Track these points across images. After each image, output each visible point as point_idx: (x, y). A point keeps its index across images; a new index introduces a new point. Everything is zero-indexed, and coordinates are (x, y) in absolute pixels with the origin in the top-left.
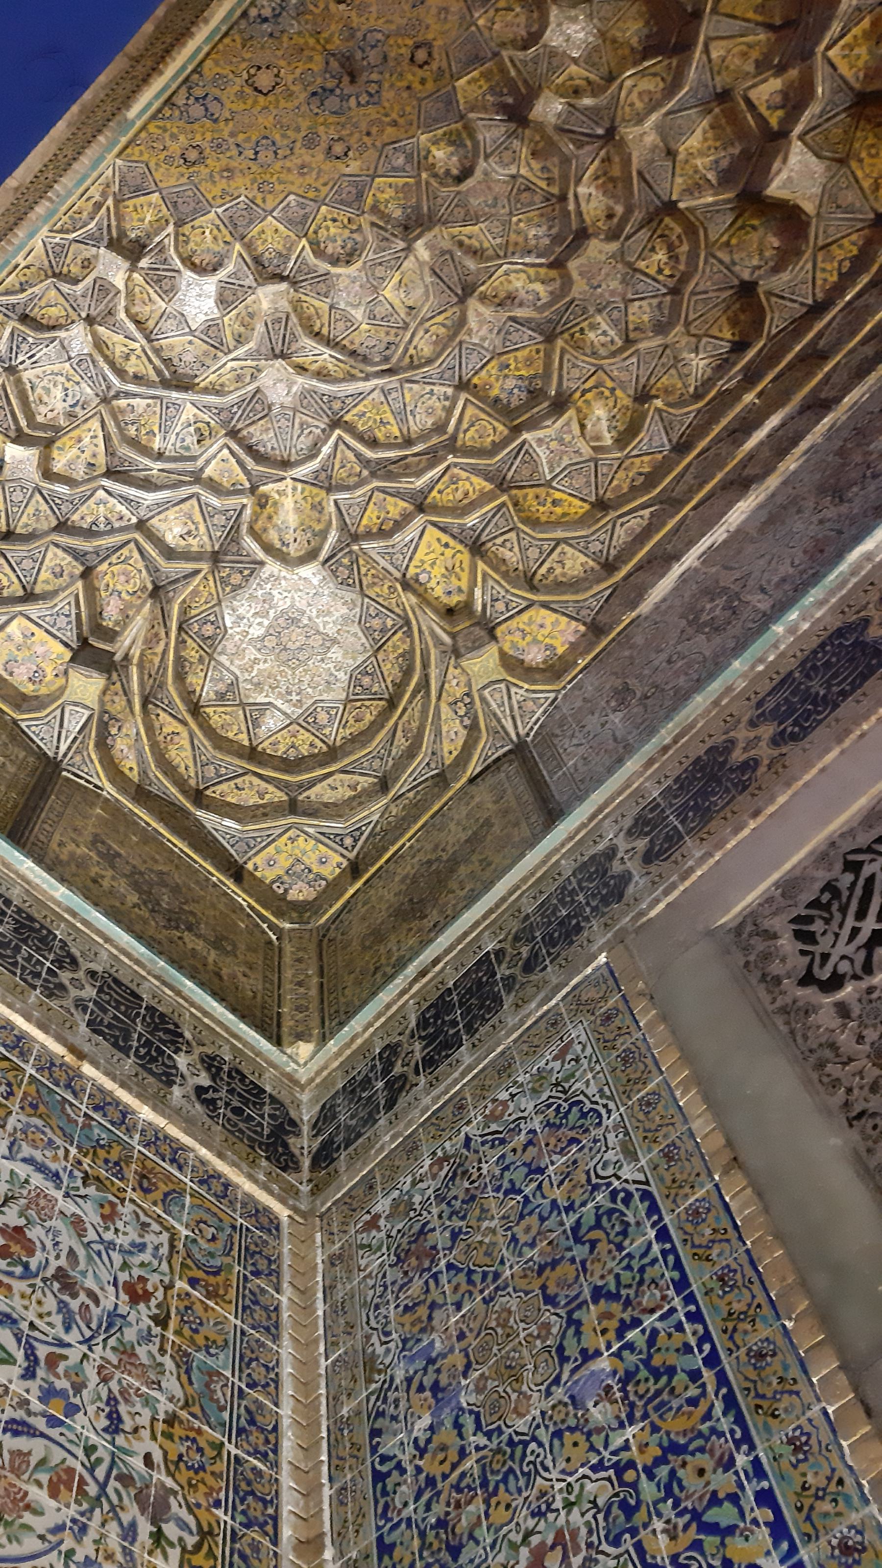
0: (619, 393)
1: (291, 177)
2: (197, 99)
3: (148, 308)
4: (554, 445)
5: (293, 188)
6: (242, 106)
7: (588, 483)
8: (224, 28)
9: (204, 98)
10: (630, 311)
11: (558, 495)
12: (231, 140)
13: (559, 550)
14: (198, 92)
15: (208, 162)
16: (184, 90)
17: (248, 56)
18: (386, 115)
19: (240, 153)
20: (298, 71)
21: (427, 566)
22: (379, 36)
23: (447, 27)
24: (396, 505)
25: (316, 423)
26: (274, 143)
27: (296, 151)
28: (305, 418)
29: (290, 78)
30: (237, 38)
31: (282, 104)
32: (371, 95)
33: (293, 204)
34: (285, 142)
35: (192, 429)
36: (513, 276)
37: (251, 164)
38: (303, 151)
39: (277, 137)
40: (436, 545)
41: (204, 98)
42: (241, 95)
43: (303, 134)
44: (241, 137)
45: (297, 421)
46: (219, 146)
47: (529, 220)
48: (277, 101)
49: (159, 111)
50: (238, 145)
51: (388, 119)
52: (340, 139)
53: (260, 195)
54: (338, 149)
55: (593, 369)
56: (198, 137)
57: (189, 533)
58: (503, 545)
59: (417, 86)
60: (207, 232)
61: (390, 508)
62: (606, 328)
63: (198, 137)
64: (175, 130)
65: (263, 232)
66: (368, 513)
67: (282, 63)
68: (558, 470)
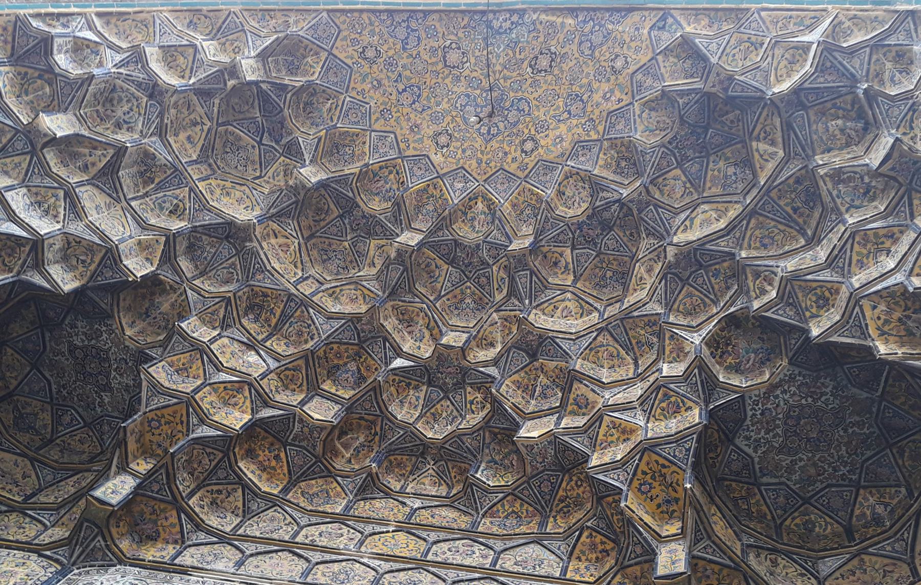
0: (377, 438)
1: (404, 124)
2: (408, 27)
3: (247, 107)
4: (306, 430)
5: (398, 132)
6: (426, 57)
7: (301, 467)
8: (463, 8)
9: (413, 30)
10: (442, 402)
11: (283, 455)
12: (400, 68)
13: (236, 486)
14: (413, 25)
15: (375, 66)
16: (406, 15)
17: (460, 34)
18: (482, 152)
19: (396, 81)
20: (475, 74)
21: (163, 421)
22: (527, 109)
23: (553, 148)
24: (198, 369)
25: (239, 272)
26: (419, 96)
27: (424, 114)
28: (238, 262)
29: (467, 72)
30: (466, 20)
31: (447, 81)
32: (489, 132)
33: (389, 139)
34: (425, 102)
35: (175, 201)
36: (422, 314)
37: (395, 93)
38: (428, 118)
39: (425, 95)
40: (178, 415)
41: (413, 30)
42: (433, 51)
43: (438, 109)
44: (408, 73)
45: (233, 259)
46: (391, 64)
47: (473, 293)
48: (447, 77)
49: (380, 11)
50: (400, 75)
51: (480, 155)
52: (450, 135)
53: (377, 115)
54: (443, 140)
55: (378, 413)
56: (385, 47)
57: (83, 262)
58: (209, 454)
59: (510, 157)
60: (330, 102)
61: (194, 367)
62: (422, 397)
63: (385, 47)
64: (377, 30)
65: (357, 135)
66: (182, 356)
67: (473, 60)
68: (297, 443)
